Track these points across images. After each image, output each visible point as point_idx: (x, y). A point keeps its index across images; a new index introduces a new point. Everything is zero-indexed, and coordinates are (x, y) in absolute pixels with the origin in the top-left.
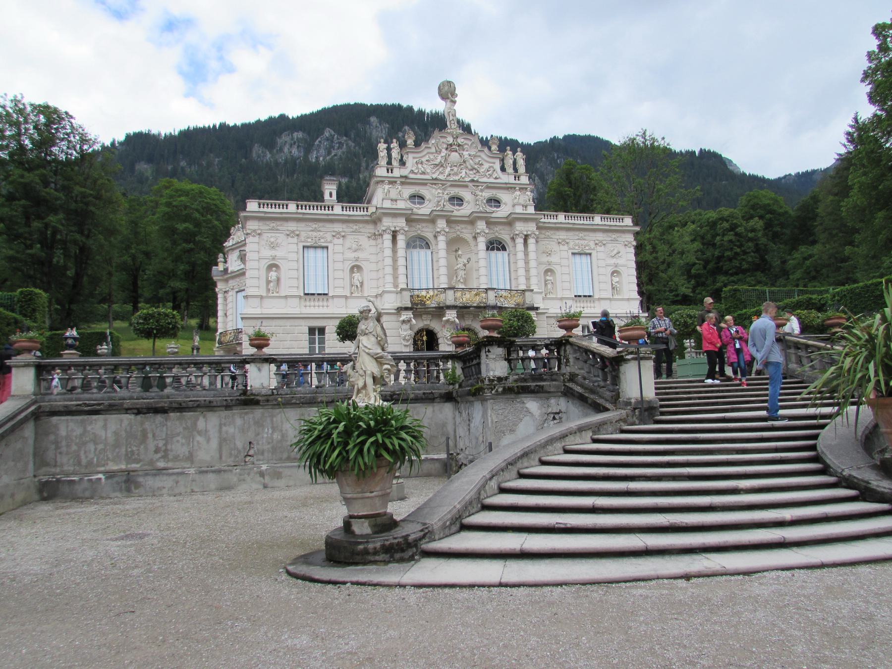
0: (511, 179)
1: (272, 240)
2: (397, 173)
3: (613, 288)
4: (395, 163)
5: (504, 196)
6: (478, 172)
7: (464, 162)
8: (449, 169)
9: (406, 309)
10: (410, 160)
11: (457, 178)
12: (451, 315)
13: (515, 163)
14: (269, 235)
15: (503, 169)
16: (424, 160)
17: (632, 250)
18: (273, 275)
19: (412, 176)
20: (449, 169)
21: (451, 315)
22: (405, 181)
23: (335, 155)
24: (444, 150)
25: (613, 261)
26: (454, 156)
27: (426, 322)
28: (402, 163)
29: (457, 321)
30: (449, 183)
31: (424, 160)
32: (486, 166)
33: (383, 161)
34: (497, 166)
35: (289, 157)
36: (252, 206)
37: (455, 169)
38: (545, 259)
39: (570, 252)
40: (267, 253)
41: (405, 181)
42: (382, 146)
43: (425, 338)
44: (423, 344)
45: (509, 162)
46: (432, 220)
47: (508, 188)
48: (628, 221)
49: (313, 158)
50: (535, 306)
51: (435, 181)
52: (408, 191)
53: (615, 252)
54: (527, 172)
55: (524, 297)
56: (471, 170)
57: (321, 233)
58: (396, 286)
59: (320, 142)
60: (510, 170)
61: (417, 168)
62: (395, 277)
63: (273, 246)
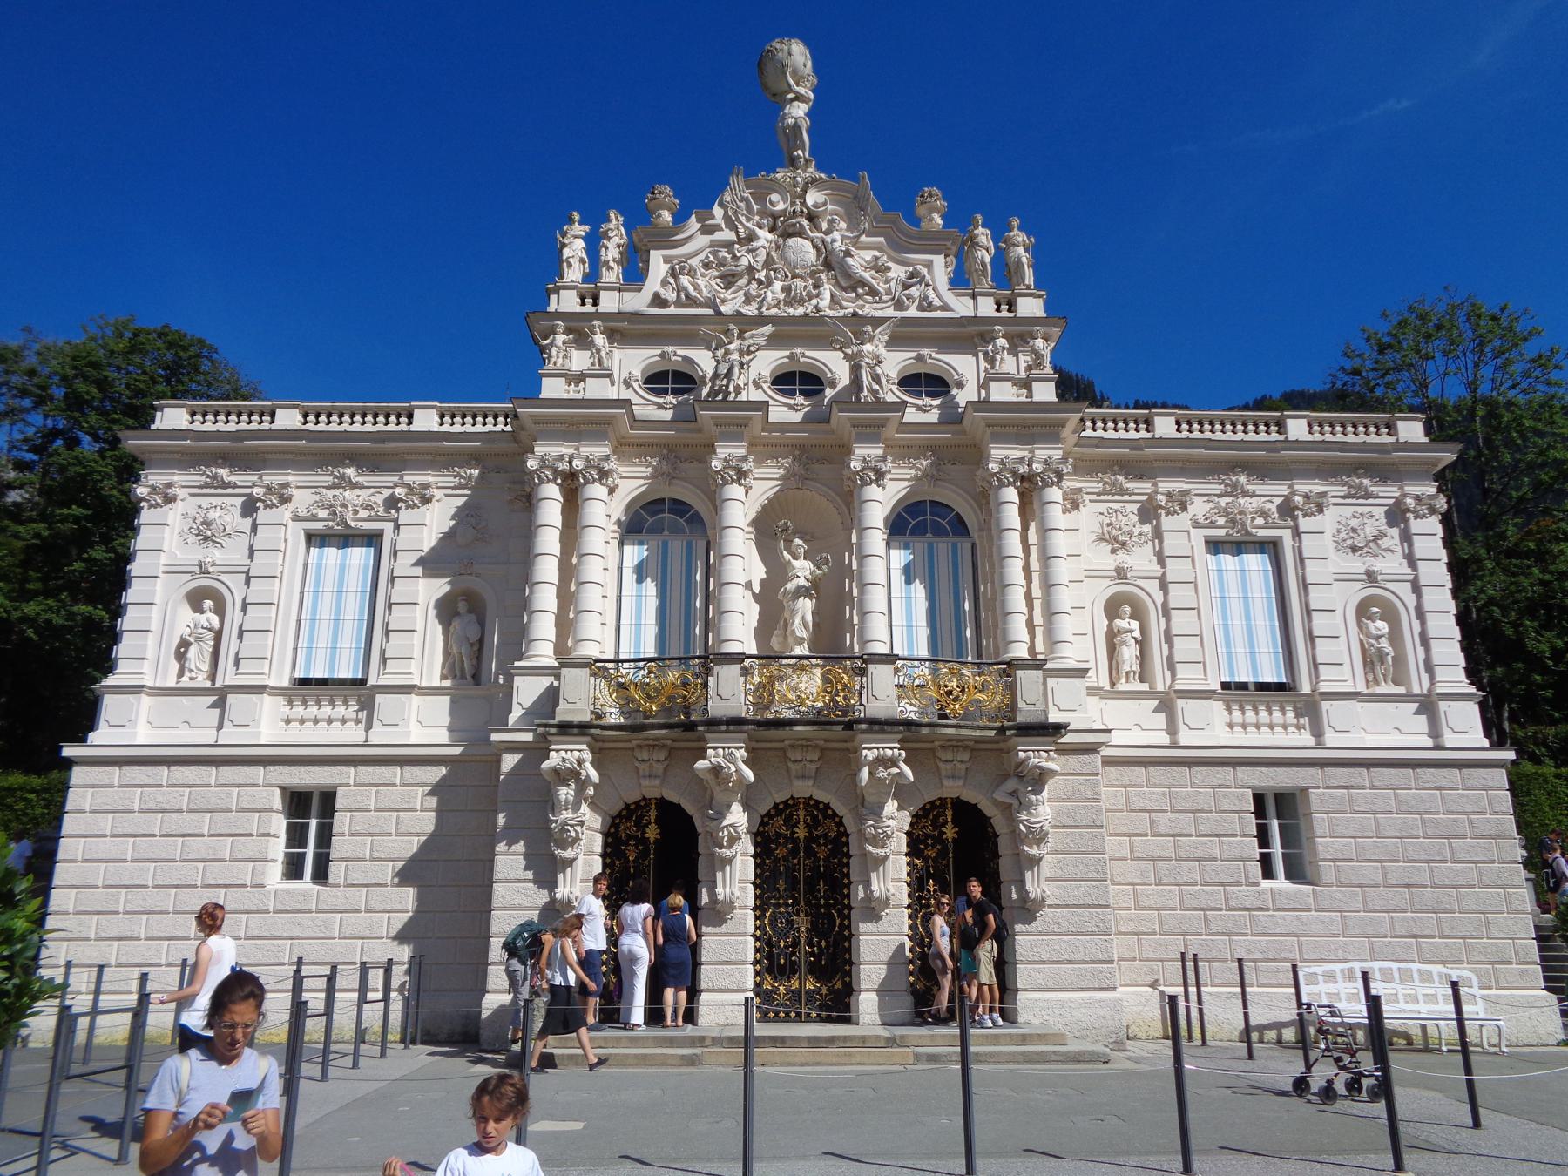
0: (987, 307)
1: (213, 515)
2: (610, 302)
3: (1371, 660)
5: (964, 366)
6: (873, 292)
7: (828, 265)
8: (778, 286)
10: (658, 265)
11: (800, 311)
14: (205, 502)
15: (960, 280)
16: (694, 262)
17: (1434, 525)
20: (778, 286)
24: (760, 232)
25: (1357, 565)
28: (635, 274)
29: (749, 774)
30: (768, 329)
31: (694, 262)
32: (898, 272)
36: (173, 417)
37: (799, 283)
39: (1198, 537)
40: (193, 554)
43: (652, 833)
44: (644, 855)
47: (970, 336)
48: (1412, 430)
50: (1054, 717)
52: (634, 361)
53: (1370, 531)
54: (1039, 284)
55: (1011, 689)
56: (854, 290)
57: (364, 493)
60: (986, 284)
61: (679, 289)
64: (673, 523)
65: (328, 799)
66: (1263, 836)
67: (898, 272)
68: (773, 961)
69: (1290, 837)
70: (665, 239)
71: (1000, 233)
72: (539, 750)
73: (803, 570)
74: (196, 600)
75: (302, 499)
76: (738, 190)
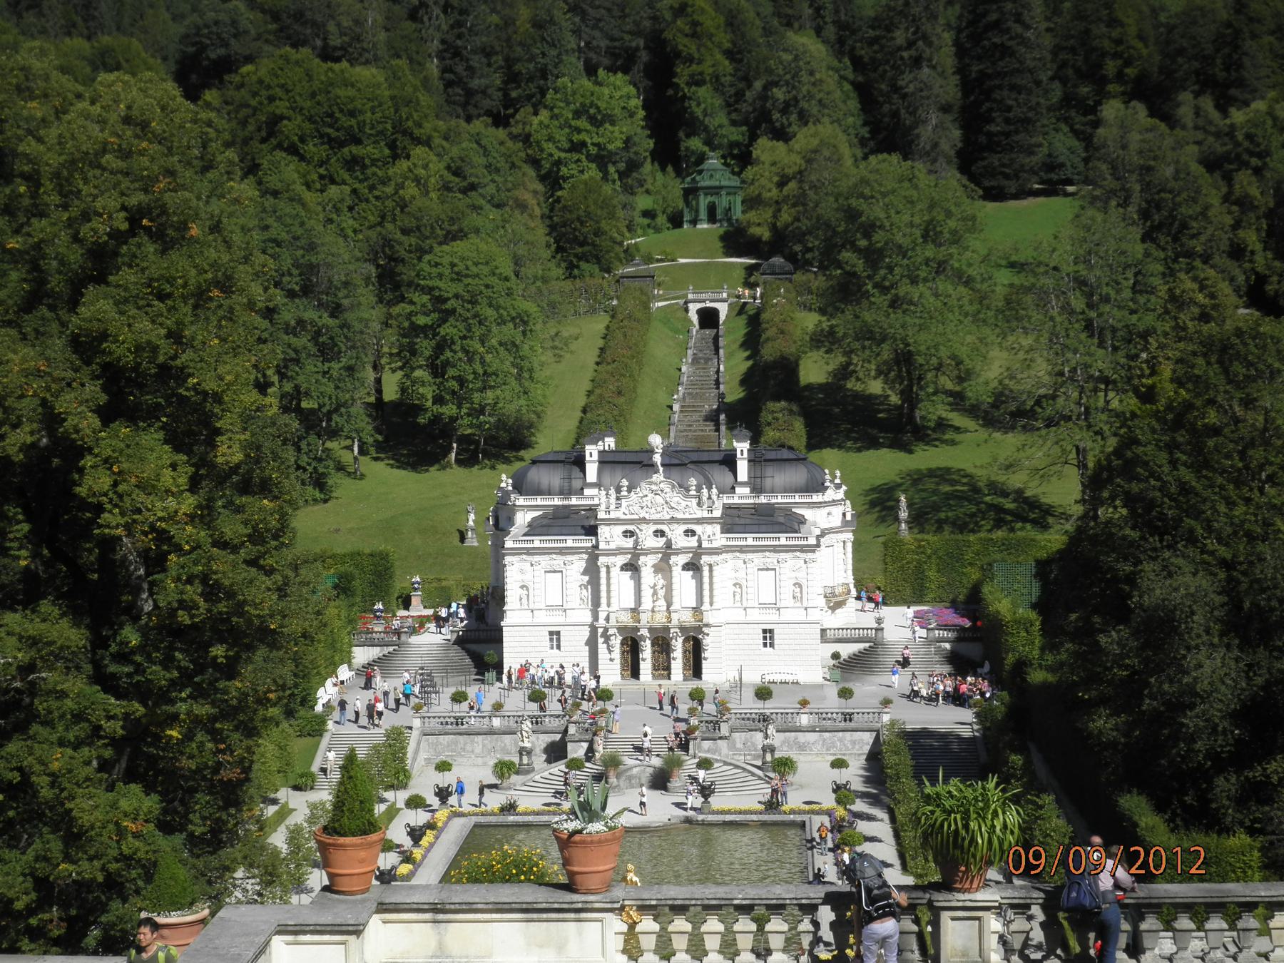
2: (613, 515)
4: (612, 507)
9: (612, 627)
13: (710, 498)
15: (699, 504)
19: (624, 517)
22: (617, 522)
25: (794, 575)
26: (659, 499)
28: (618, 506)
32: (684, 504)
33: (603, 507)
34: (695, 501)
38: (733, 575)
40: (520, 577)
41: (617, 522)
45: (705, 499)
47: (699, 521)
51: (644, 520)
58: (609, 605)
62: (609, 598)
63: (522, 571)
64: (632, 567)
65: (558, 633)
66: (765, 638)
67: (684, 504)
68: (655, 668)
69: (771, 638)
70: (625, 497)
71: (710, 488)
72: (606, 630)
73: (661, 582)
74: (522, 587)
75: (543, 563)
76: (643, 484)
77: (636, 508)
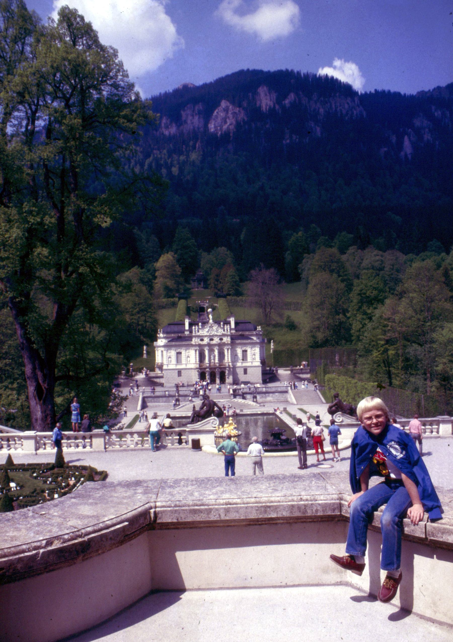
12: (208, 370)
15: (224, 330)
18: (170, 359)
21: (208, 370)
23: (230, 124)
27: (203, 371)
28: (198, 331)
35: (192, 127)
40: (169, 354)
41: (199, 336)
42: (194, 327)
45: (226, 329)
46: (205, 345)
49: (212, 127)
51: (206, 336)
59: (217, 113)
77: (205, 332)
